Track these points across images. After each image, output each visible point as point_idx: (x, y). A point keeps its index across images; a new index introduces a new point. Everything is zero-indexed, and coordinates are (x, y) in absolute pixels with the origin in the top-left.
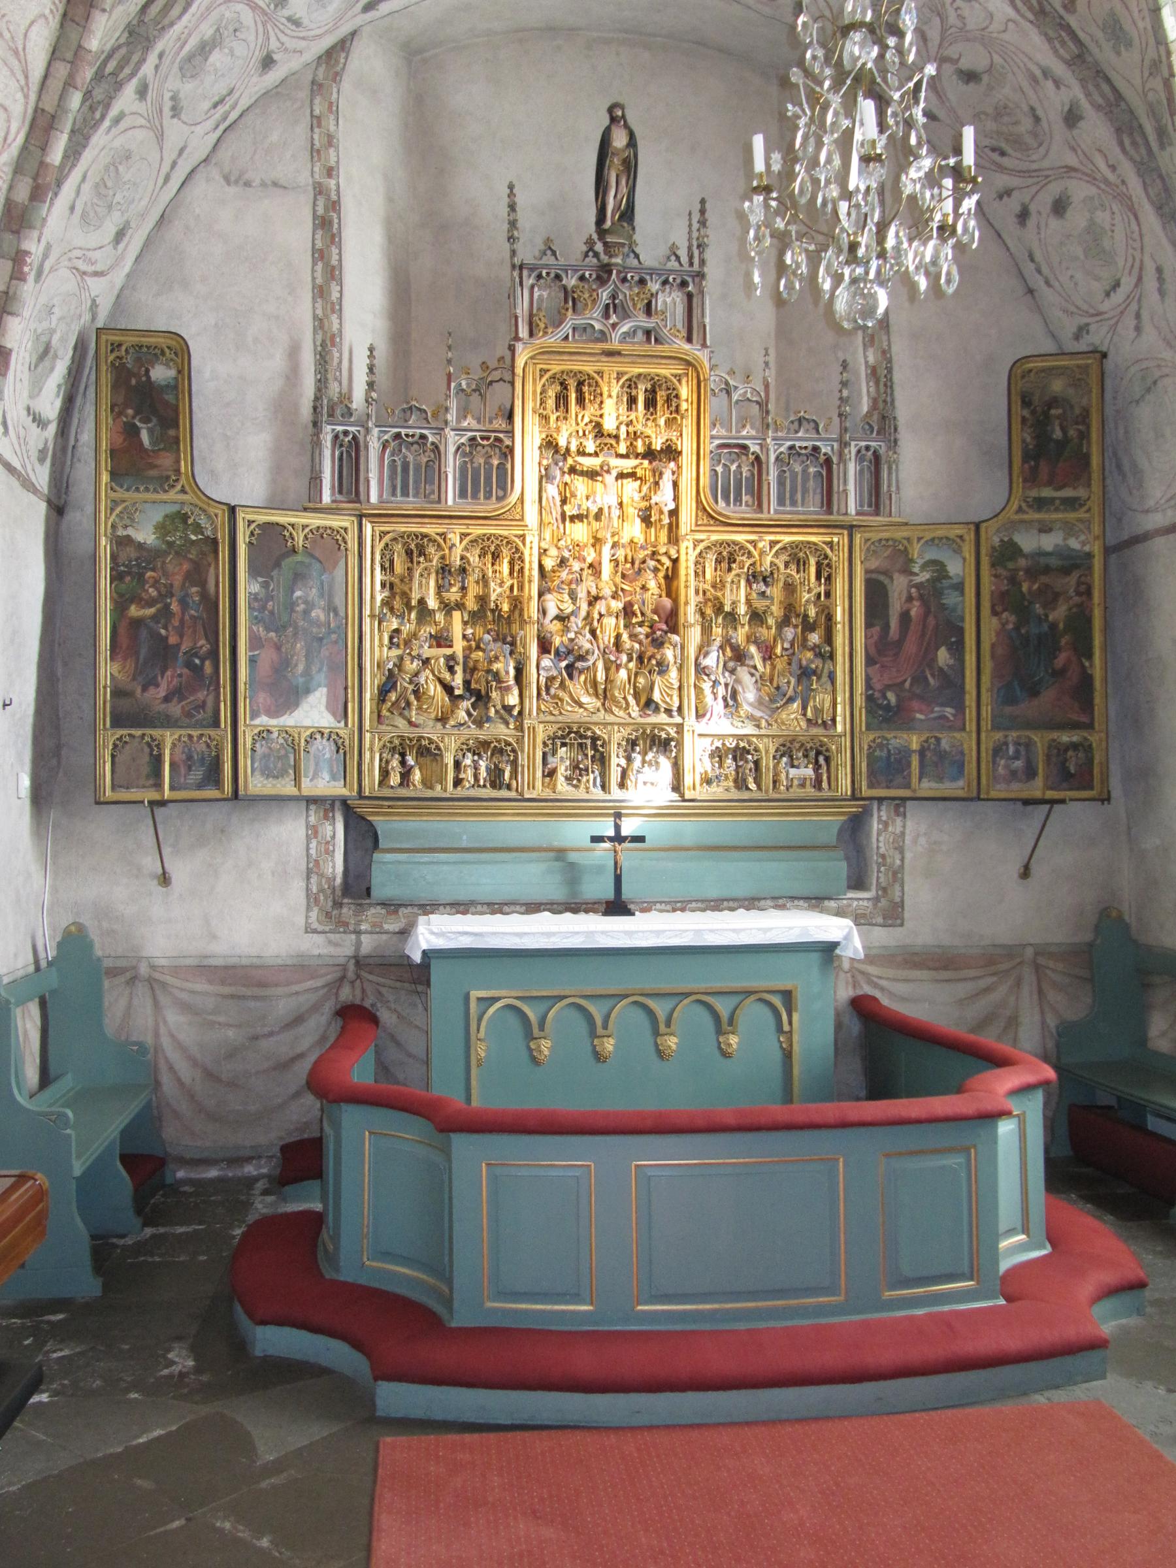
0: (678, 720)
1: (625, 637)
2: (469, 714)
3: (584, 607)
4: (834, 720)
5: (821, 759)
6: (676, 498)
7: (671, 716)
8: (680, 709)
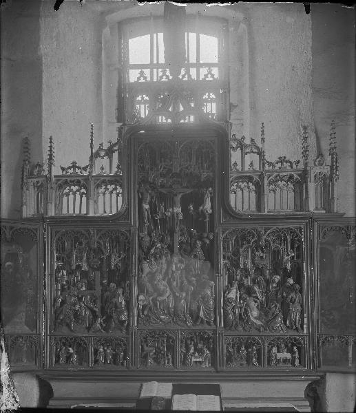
0: (214, 327)
1: (186, 282)
3: (165, 266)
4: (302, 327)
5: (295, 348)
6: (212, 207)
7: (210, 325)
8: (215, 321)
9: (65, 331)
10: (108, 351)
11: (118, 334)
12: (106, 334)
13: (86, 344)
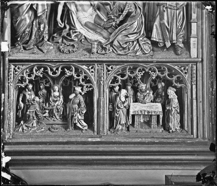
5: (171, 92)
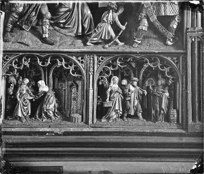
2: (117, 30)
9: (30, 42)
10: (132, 88)
11: (155, 47)
12: (127, 49)
13: (79, 72)
